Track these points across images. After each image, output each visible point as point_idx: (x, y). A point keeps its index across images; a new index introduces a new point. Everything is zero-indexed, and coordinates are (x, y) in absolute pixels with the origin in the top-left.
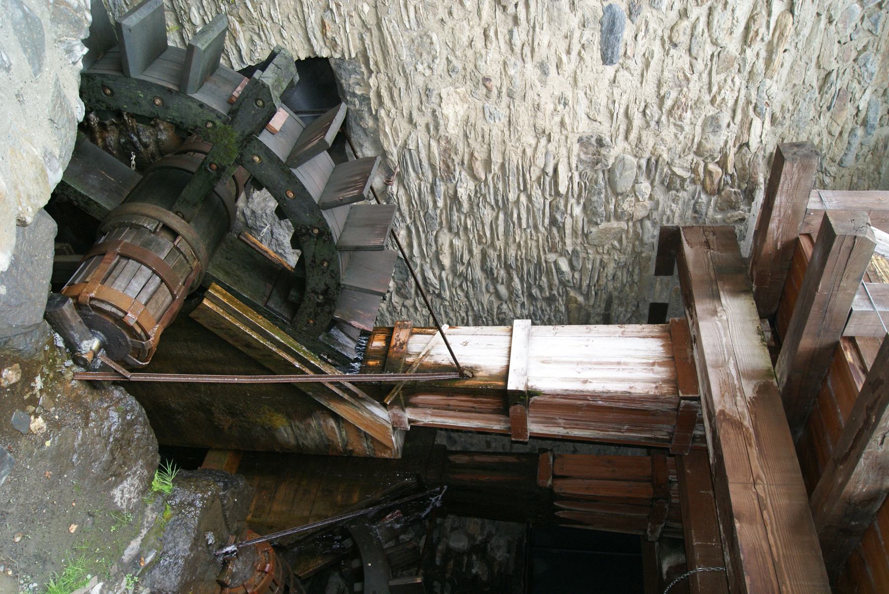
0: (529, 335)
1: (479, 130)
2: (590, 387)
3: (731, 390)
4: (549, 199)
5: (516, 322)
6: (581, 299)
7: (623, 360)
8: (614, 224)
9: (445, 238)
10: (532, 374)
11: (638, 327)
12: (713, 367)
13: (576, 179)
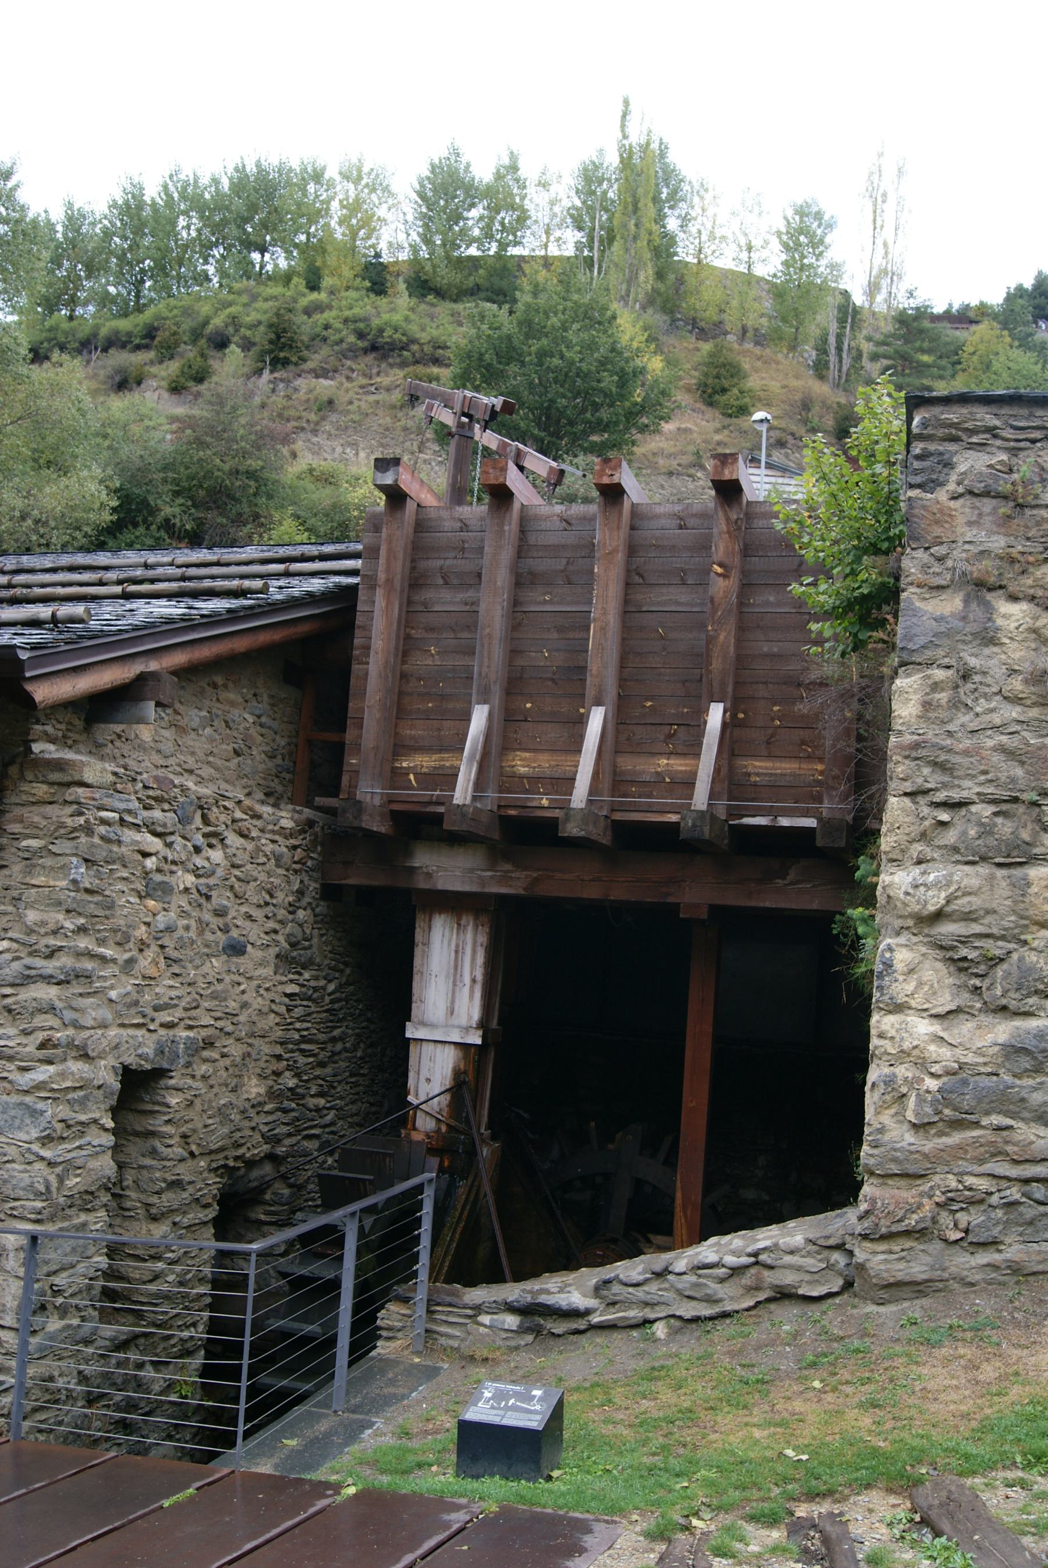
0: (423, 1024)
1: (263, 1065)
2: (479, 977)
3: (505, 879)
4: (299, 1002)
5: (408, 1035)
6: (348, 971)
7: (453, 947)
8: (315, 941)
9: (312, 1102)
10: (464, 1022)
11: (418, 931)
12: (484, 886)
13: (291, 976)
